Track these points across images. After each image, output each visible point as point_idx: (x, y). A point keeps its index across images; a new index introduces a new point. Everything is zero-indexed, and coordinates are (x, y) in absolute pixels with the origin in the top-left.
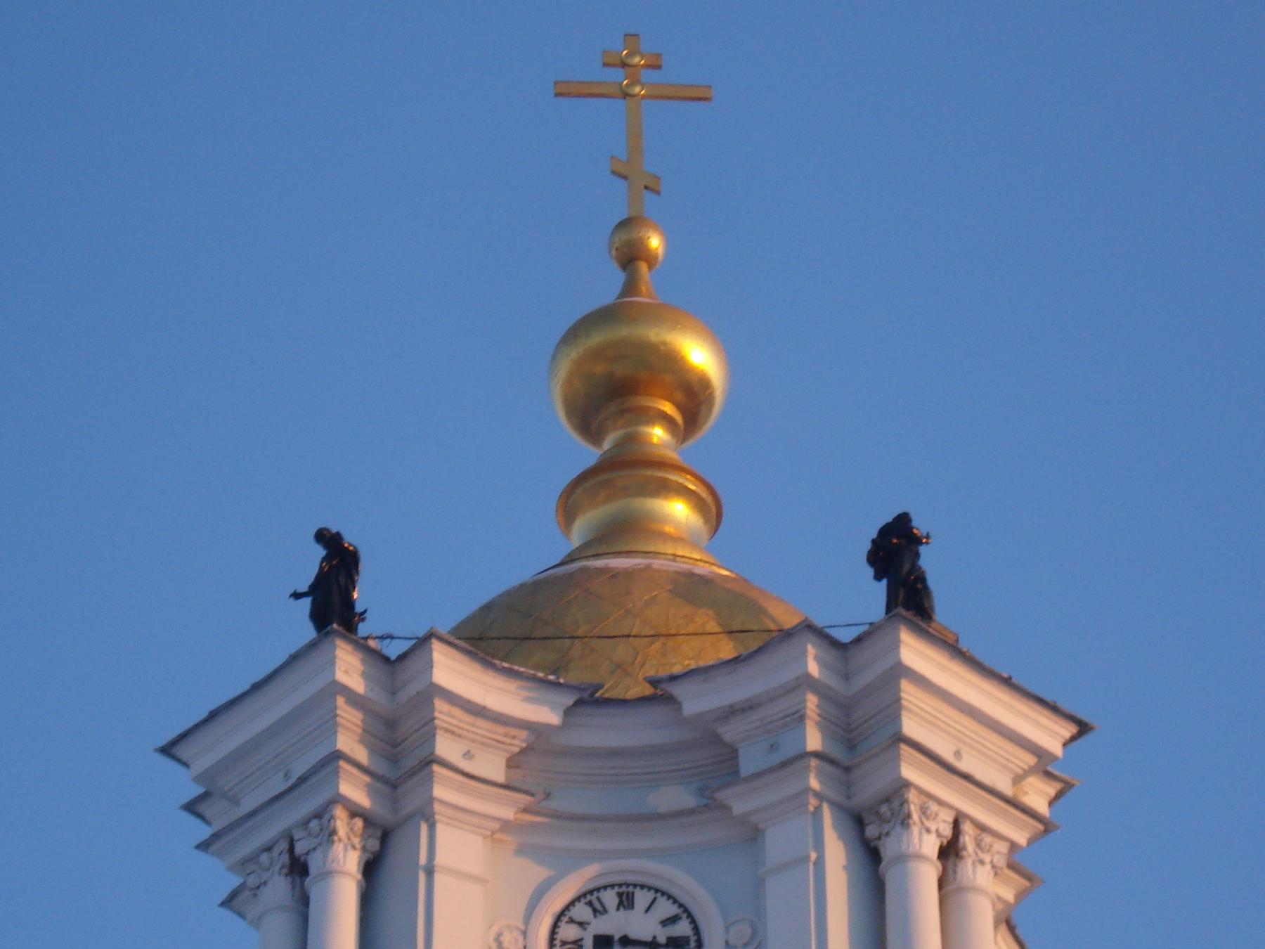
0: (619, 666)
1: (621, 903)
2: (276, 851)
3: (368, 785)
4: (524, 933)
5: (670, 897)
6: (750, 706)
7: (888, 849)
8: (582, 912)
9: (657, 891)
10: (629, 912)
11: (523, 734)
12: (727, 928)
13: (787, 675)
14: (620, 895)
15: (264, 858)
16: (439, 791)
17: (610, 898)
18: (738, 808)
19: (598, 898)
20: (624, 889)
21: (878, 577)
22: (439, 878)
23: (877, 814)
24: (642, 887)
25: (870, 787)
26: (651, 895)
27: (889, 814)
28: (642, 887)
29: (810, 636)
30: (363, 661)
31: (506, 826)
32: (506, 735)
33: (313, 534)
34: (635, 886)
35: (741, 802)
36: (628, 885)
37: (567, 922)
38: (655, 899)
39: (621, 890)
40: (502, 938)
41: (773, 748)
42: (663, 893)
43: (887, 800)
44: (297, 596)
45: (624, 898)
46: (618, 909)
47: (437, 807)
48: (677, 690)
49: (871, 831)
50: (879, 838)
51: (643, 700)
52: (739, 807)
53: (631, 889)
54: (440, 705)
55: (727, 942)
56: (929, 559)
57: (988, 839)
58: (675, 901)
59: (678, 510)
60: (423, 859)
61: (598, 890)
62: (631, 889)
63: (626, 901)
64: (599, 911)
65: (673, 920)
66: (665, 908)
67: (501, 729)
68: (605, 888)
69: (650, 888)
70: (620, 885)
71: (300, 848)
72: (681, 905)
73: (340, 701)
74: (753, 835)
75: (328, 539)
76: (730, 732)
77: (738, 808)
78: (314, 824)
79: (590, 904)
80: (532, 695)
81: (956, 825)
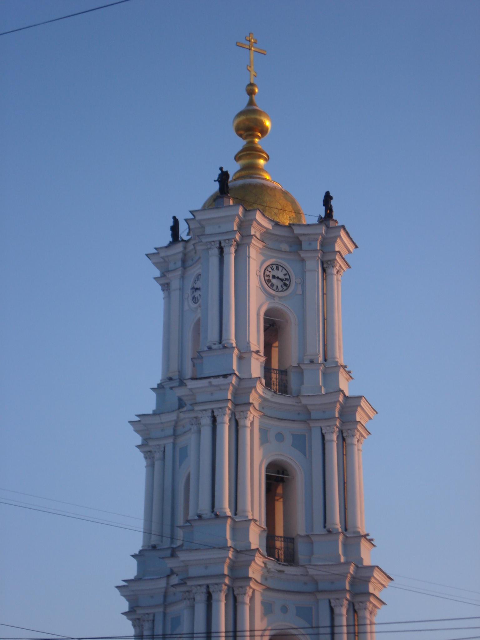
0: (275, 214)
3: (240, 237)
4: (259, 271)
7: (329, 271)
8: (269, 269)
10: (278, 271)
11: (265, 230)
12: (296, 279)
13: (318, 231)
15: (213, 243)
16: (253, 241)
17: (274, 267)
22: (251, 259)
23: (327, 263)
24: (280, 266)
25: (328, 257)
27: (330, 264)
28: (280, 266)
29: (325, 226)
30: (243, 210)
31: (260, 249)
32: (262, 229)
34: (279, 265)
36: (277, 265)
41: (310, 244)
42: (284, 268)
43: (330, 261)
44: (215, 181)
47: (251, 244)
48: (293, 227)
50: (326, 267)
52: (302, 255)
54: (254, 222)
55: (296, 282)
56: (333, 203)
58: (286, 270)
59: (262, 162)
60: (248, 255)
61: (272, 264)
62: (278, 266)
63: (277, 269)
64: (273, 270)
66: (285, 272)
67: (261, 228)
71: (223, 245)
72: (287, 272)
73: (237, 217)
74: (303, 260)
75: (221, 169)
76: (301, 238)
78: (227, 241)
79: (271, 267)
80: (268, 222)
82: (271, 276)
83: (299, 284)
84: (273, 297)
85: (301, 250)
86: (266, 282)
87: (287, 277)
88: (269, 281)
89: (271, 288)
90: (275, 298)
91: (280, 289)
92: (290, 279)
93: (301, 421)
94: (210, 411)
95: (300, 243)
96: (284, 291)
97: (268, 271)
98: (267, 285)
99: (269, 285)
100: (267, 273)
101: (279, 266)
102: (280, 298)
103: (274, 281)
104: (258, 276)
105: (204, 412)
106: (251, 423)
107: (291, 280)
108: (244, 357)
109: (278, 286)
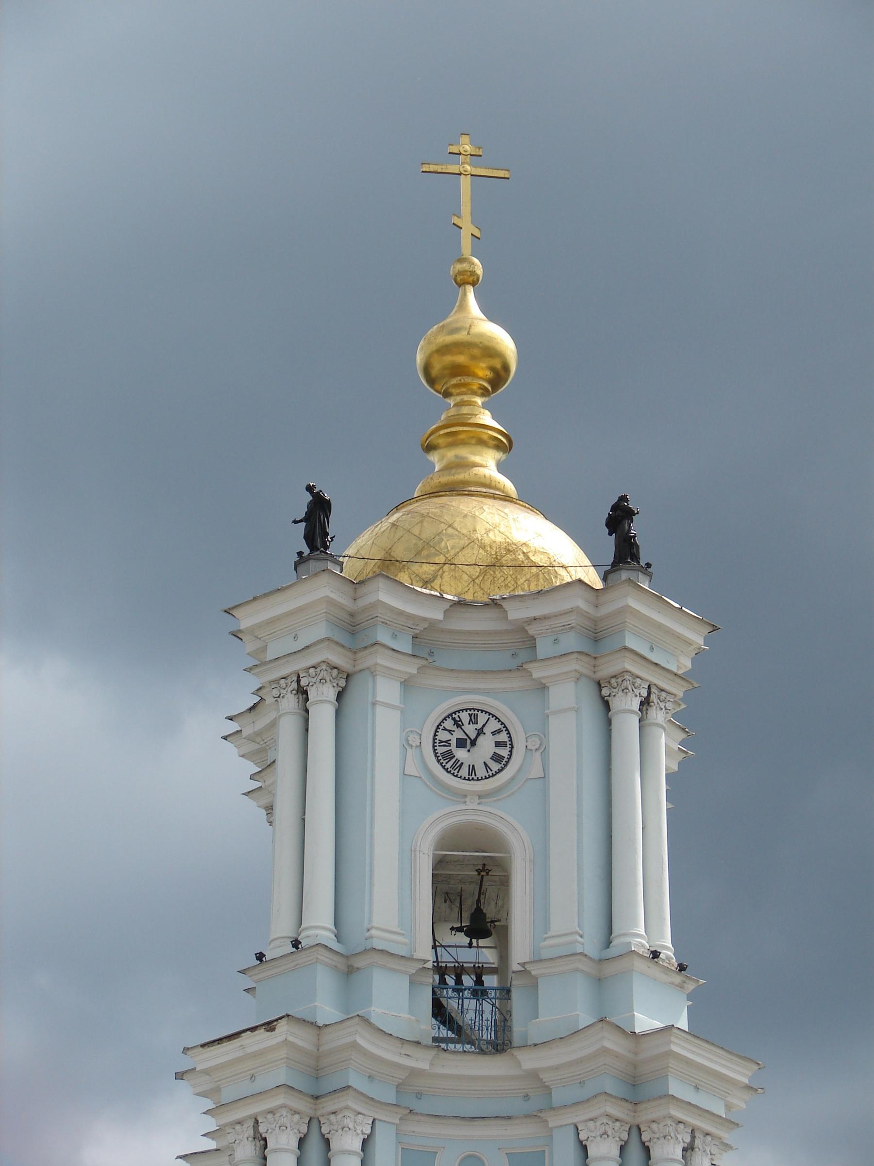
1: (471, 720)
2: (289, 681)
5: (497, 718)
6: (545, 618)
9: (490, 714)
12: (526, 738)
14: (470, 715)
18: (535, 675)
19: (459, 716)
20: (472, 712)
21: (610, 534)
24: (482, 711)
26: (487, 716)
28: (482, 711)
33: (305, 490)
34: (478, 710)
35: (538, 672)
36: (474, 710)
37: (442, 729)
38: (489, 718)
39: (471, 713)
40: (409, 738)
45: (473, 717)
46: (469, 724)
48: (504, 604)
49: (605, 692)
51: (486, 605)
53: (476, 712)
55: (526, 747)
57: (664, 694)
60: (370, 699)
61: (459, 711)
62: (476, 712)
64: (458, 724)
65: (499, 731)
68: (462, 710)
70: (470, 710)
71: (303, 682)
72: (503, 723)
74: (542, 688)
76: (532, 630)
77: (535, 675)
78: (312, 670)
81: (649, 687)
82: (454, 743)
84: (464, 796)
85: (534, 660)
86: (438, 761)
88: (449, 755)
89: (453, 774)
90: (468, 799)
91: (481, 772)
92: (511, 740)
93: (527, 1116)
94: (251, 1123)
95: (531, 643)
96: (493, 775)
97: (445, 729)
98: (444, 767)
99: (448, 766)
100: (443, 736)
101: (479, 713)
102: (481, 796)
103: (461, 754)
105: (238, 1127)
106: (364, 1141)
107: (515, 745)
108: (358, 969)
109: (473, 766)
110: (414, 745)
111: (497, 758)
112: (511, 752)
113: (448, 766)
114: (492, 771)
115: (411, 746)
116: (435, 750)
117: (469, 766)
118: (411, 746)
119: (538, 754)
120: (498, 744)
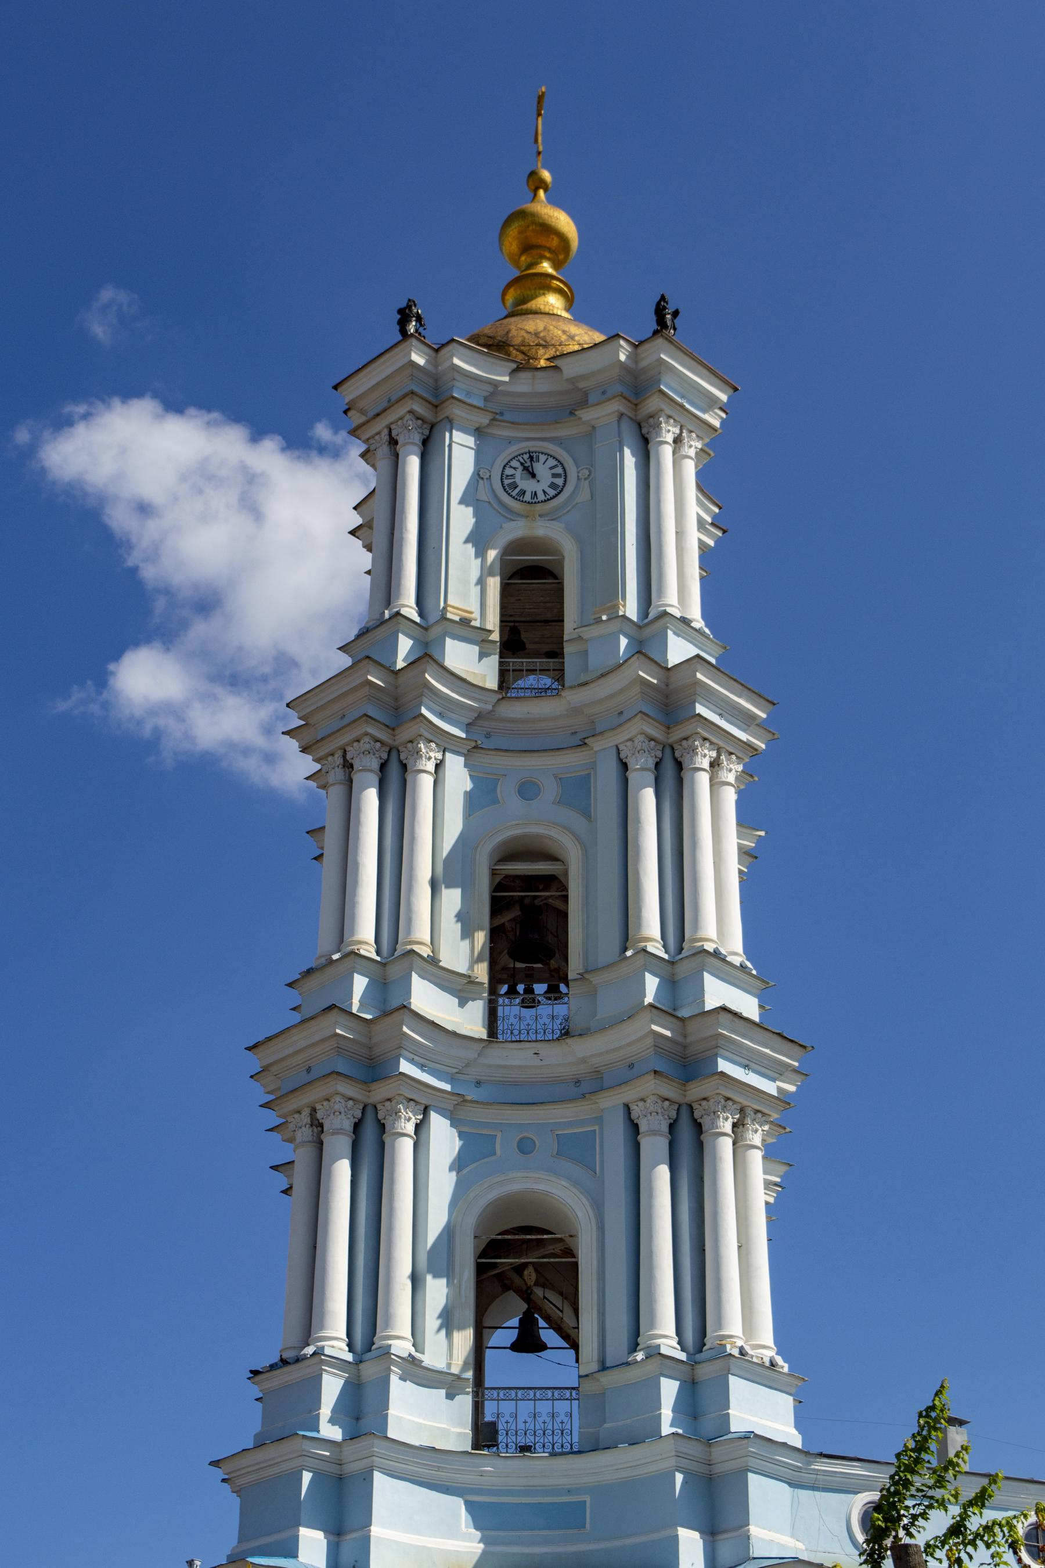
5: (554, 458)
8: (515, 464)
9: (548, 455)
26: (546, 457)
28: (542, 453)
34: (539, 453)
38: (547, 459)
40: (480, 473)
42: (551, 456)
58: (557, 460)
60: (447, 442)
66: (552, 462)
69: (545, 454)
72: (559, 461)
79: (519, 461)
83: (585, 479)
86: (505, 490)
87: (559, 470)
88: (514, 486)
97: (511, 467)
98: (509, 494)
99: (514, 493)
104: (485, 480)
109: (535, 492)
110: (485, 477)
111: (553, 486)
112: (565, 481)
113: (514, 493)
114: (549, 495)
115: (482, 478)
116: (502, 482)
117: (532, 492)
118: (482, 478)
119: (587, 482)
120: (555, 476)
